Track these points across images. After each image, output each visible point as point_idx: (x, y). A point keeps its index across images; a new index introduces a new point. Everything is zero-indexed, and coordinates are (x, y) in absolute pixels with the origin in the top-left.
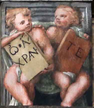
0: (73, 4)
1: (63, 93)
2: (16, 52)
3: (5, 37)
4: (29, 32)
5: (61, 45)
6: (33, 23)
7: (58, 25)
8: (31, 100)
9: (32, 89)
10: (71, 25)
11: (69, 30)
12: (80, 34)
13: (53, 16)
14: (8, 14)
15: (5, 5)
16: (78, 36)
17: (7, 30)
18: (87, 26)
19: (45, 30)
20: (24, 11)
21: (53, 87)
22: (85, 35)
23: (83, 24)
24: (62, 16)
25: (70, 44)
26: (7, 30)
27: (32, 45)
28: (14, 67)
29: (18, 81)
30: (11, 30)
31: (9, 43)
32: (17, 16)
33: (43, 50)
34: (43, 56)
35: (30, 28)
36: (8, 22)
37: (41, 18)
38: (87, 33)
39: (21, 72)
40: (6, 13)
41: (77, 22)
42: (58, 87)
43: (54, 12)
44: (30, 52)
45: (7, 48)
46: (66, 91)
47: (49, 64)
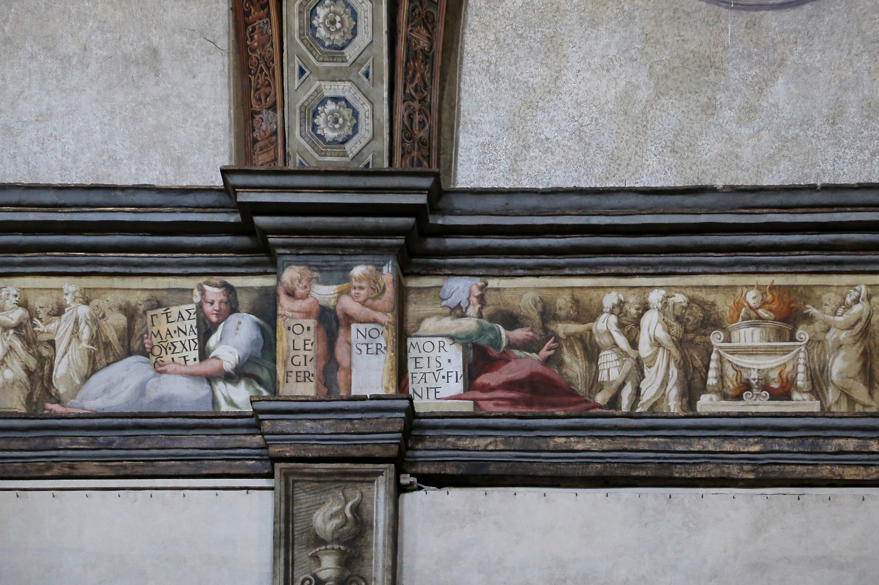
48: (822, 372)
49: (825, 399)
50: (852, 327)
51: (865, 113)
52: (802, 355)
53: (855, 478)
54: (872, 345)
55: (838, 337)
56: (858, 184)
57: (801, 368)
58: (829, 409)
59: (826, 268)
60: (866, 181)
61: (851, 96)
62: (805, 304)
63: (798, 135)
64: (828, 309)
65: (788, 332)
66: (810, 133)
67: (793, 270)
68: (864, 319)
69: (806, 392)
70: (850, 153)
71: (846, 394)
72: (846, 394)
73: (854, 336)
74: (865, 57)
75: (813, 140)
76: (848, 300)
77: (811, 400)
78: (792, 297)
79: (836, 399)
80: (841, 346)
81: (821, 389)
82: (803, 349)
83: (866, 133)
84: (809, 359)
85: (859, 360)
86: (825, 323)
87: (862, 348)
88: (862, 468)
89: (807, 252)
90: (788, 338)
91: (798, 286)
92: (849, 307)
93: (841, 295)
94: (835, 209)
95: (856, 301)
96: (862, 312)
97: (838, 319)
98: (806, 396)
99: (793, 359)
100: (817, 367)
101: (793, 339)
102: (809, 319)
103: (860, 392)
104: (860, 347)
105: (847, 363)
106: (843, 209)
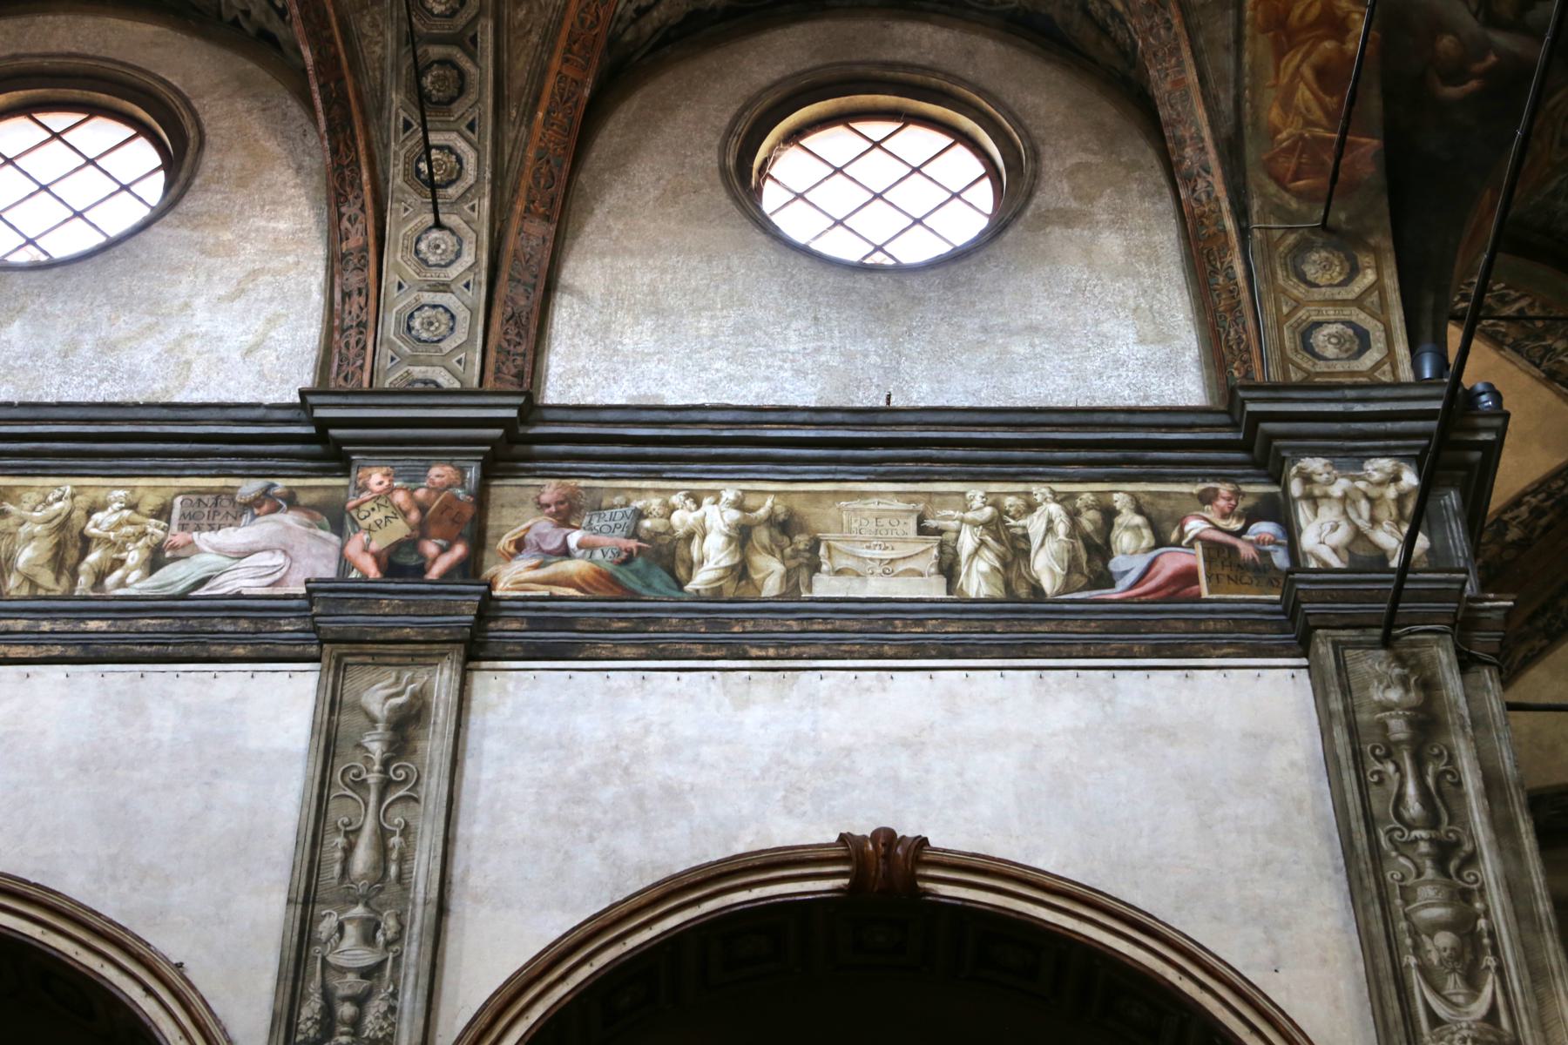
50: (50, 521)
51: (99, 350)
53: (22, 656)
54: (68, 535)
59: (29, 472)
61: (87, 336)
63: (26, 365)
64: (27, 506)
66: (39, 363)
68: (64, 514)
70: (77, 380)
74: (107, 308)
75: (41, 369)
76: (51, 498)
79: (17, 585)
80: (34, 537)
83: (97, 365)
85: (51, 549)
87: (56, 541)
88: (32, 647)
92: (51, 504)
95: (59, 499)
96: (63, 509)
97: (35, 514)
103: (46, 578)
105: (36, 553)
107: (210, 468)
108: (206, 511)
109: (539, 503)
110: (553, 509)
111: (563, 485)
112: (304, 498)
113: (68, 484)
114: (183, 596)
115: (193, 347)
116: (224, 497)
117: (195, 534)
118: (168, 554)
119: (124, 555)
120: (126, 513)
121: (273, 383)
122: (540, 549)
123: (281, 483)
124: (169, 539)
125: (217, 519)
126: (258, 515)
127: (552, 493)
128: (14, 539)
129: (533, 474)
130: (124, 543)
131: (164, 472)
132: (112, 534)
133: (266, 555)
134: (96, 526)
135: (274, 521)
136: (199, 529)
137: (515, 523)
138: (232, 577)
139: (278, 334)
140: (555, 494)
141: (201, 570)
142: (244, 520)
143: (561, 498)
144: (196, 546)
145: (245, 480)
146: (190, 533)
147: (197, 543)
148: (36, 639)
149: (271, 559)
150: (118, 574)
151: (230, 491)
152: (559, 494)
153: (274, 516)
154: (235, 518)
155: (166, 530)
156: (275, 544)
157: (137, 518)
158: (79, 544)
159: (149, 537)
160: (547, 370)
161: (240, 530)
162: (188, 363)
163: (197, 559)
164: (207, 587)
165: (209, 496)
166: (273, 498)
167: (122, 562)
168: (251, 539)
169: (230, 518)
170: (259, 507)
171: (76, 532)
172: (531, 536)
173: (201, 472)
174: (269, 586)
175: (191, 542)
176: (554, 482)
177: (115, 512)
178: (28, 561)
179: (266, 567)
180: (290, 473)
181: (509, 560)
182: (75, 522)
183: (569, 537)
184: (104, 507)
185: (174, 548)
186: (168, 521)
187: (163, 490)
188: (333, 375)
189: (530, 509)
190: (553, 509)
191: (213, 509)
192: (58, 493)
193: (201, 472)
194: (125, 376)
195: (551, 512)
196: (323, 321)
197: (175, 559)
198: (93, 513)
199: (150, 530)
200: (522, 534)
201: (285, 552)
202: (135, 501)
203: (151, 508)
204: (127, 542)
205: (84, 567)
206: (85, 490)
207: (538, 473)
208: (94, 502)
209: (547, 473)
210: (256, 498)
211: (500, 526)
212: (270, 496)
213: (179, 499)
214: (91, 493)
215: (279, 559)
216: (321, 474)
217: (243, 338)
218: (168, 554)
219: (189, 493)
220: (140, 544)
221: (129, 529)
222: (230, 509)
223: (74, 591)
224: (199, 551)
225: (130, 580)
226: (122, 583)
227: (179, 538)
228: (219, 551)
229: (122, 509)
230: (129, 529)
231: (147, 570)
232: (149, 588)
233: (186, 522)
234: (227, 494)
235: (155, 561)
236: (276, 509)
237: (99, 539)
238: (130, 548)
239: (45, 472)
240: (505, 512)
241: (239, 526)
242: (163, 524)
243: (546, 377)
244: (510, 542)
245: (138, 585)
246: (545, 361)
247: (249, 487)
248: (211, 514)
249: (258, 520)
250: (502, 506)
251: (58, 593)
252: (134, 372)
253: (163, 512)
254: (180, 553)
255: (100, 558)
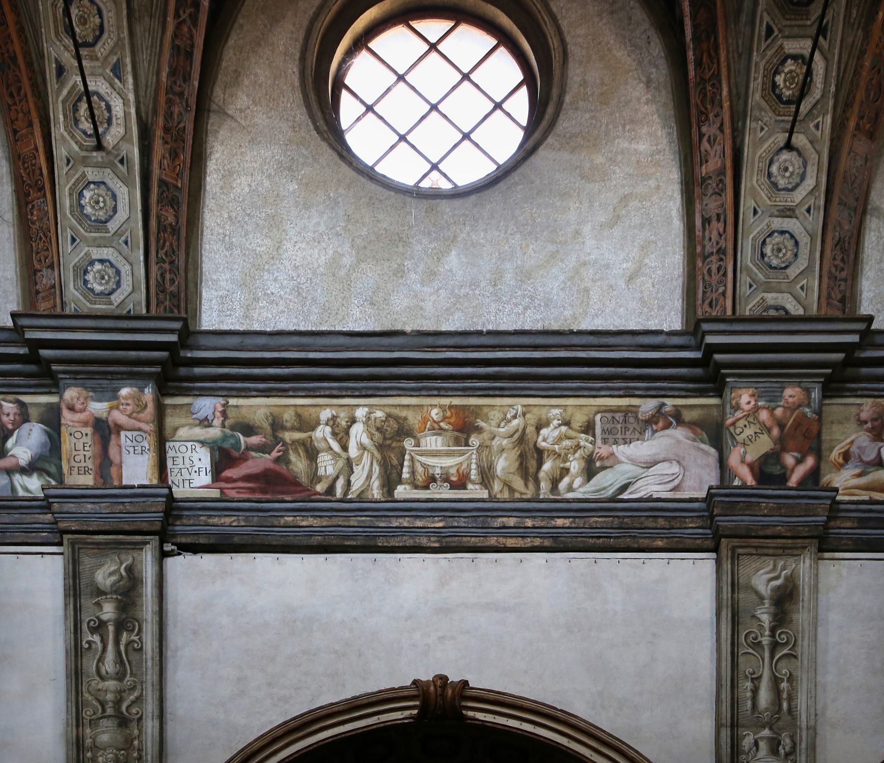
0: (803, 385)
1: (788, 473)
2: (741, 433)
3: (730, 418)
4: (755, 412)
5: (788, 426)
6: (760, 404)
7: (786, 405)
8: (755, 480)
9: (756, 469)
10: (799, 406)
11: (797, 411)
12: (809, 415)
13: (781, 396)
14: (733, 395)
15: (730, 385)
16: (807, 417)
17: (732, 411)
18: (817, 406)
19: (772, 410)
20: (751, 391)
21: (779, 467)
22: (814, 415)
23: (812, 404)
24: (791, 396)
25: (797, 425)
26: (732, 411)
27: (758, 426)
28: (739, 448)
29: (743, 461)
30: (736, 411)
31: (733, 424)
32: (743, 397)
33: (769, 430)
34: (770, 437)
35: (757, 409)
36: (734, 402)
37: (768, 399)
38: (816, 414)
39: (745, 453)
40: (731, 393)
41: (806, 402)
42: (784, 467)
43: (782, 392)
44: (755, 433)
45: (732, 429)
46: (792, 470)
47: (775, 445)
48: (490, 468)
49: (492, 489)
50: (512, 436)
52: (474, 456)
54: (527, 449)
55: (501, 444)
56: (515, 330)
57: (474, 466)
58: (495, 496)
59: (491, 393)
60: (520, 328)
62: (476, 419)
64: (494, 423)
65: (463, 440)
67: (466, 394)
68: (520, 431)
69: (478, 484)
71: (507, 485)
72: (507, 485)
73: (513, 443)
76: (509, 416)
77: (481, 489)
78: (466, 414)
80: (503, 450)
81: (489, 482)
82: (475, 452)
84: (479, 460)
85: (517, 460)
86: (492, 433)
87: (519, 451)
89: (477, 381)
90: (463, 444)
91: (470, 406)
92: (509, 421)
93: (503, 413)
94: (498, 349)
95: (515, 417)
96: (519, 425)
97: (501, 430)
98: (477, 487)
99: (467, 459)
100: (486, 465)
101: (467, 445)
102: (479, 430)
103: (518, 483)
104: (518, 451)
105: (507, 463)
106: (503, 349)
107: (619, 389)
108: (619, 426)
109: (859, 420)
110: (869, 425)
111: (877, 404)
112: (687, 416)
113: (519, 403)
114: (613, 499)
115: (588, 273)
116: (630, 415)
117: (614, 447)
118: (598, 464)
119: (568, 464)
120: (564, 429)
121: (652, 309)
122: (861, 460)
123: (669, 402)
124: (596, 452)
125: (628, 435)
126: (656, 431)
127: (869, 411)
128: (490, 451)
129: (854, 393)
130: (566, 455)
131: (586, 393)
132: (556, 446)
133: (666, 465)
134: (544, 440)
135: (668, 436)
136: (616, 443)
137: (842, 438)
138: (646, 483)
139: (651, 261)
140: (871, 412)
141: (622, 478)
142: (647, 435)
143: (875, 416)
144: (616, 457)
145: (643, 400)
146: (610, 446)
147: (616, 454)
148: (521, 531)
149: (670, 468)
150: (566, 480)
151: (633, 409)
152: (874, 412)
153: (667, 432)
154: (640, 433)
155: (593, 443)
156: (672, 457)
157: (571, 433)
158: (535, 455)
159: (582, 449)
160: (861, 295)
161: (645, 444)
162: (587, 290)
163: (619, 468)
164: (629, 491)
165: (619, 414)
166: (665, 416)
167: (567, 471)
168: (654, 451)
169: (637, 433)
170: (656, 423)
171: (531, 446)
172: (854, 449)
173: (612, 393)
174: (670, 491)
175: (612, 454)
176: (870, 401)
177: (556, 428)
178: (503, 469)
179: (667, 475)
180: (676, 393)
181: (839, 470)
182: (529, 436)
183: (882, 449)
184: (547, 424)
185: (601, 459)
186: (594, 436)
187: (585, 409)
188: (700, 302)
189: (852, 426)
190: (869, 425)
191: (624, 425)
192: (513, 412)
193: (612, 393)
194: (542, 304)
195: (868, 428)
196: (684, 247)
197: (604, 468)
198: (541, 429)
199: (582, 443)
200: (848, 447)
201: (678, 462)
202: (568, 418)
203: (580, 425)
204: (568, 454)
205: (542, 475)
206: (531, 408)
207: (859, 393)
208: (540, 419)
209: (866, 393)
210: (653, 416)
211: (831, 440)
212: (663, 414)
213: (598, 417)
214: (535, 410)
215: (675, 469)
216: (698, 394)
217: (624, 266)
218: (598, 464)
219: (605, 411)
220: (577, 455)
221: (567, 443)
222: (635, 425)
223: (539, 495)
224: (620, 462)
225: (576, 484)
226: (570, 489)
227: (603, 450)
228: (633, 462)
229: (560, 425)
230: (567, 443)
231: (586, 478)
232: (589, 492)
233: (606, 436)
234: (632, 412)
235: (590, 472)
236: (668, 426)
237: (548, 451)
238: (571, 459)
239: (501, 393)
240: (835, 427)
241: (644, 440)
242: (591, 438)
243: (860, 302)
244: (839, 454)
245: (581, 490)
246: (859, 286)
247: (647, 406)
248: (623, 430)
249: (657, 434)
250: (832, 423)
251: (529, 497)
252: (548, 299)
253: (589, 428)
254: (607, 463)
255: (552, 467)
